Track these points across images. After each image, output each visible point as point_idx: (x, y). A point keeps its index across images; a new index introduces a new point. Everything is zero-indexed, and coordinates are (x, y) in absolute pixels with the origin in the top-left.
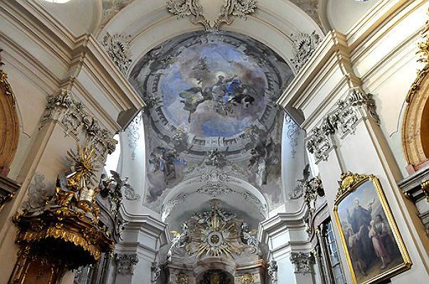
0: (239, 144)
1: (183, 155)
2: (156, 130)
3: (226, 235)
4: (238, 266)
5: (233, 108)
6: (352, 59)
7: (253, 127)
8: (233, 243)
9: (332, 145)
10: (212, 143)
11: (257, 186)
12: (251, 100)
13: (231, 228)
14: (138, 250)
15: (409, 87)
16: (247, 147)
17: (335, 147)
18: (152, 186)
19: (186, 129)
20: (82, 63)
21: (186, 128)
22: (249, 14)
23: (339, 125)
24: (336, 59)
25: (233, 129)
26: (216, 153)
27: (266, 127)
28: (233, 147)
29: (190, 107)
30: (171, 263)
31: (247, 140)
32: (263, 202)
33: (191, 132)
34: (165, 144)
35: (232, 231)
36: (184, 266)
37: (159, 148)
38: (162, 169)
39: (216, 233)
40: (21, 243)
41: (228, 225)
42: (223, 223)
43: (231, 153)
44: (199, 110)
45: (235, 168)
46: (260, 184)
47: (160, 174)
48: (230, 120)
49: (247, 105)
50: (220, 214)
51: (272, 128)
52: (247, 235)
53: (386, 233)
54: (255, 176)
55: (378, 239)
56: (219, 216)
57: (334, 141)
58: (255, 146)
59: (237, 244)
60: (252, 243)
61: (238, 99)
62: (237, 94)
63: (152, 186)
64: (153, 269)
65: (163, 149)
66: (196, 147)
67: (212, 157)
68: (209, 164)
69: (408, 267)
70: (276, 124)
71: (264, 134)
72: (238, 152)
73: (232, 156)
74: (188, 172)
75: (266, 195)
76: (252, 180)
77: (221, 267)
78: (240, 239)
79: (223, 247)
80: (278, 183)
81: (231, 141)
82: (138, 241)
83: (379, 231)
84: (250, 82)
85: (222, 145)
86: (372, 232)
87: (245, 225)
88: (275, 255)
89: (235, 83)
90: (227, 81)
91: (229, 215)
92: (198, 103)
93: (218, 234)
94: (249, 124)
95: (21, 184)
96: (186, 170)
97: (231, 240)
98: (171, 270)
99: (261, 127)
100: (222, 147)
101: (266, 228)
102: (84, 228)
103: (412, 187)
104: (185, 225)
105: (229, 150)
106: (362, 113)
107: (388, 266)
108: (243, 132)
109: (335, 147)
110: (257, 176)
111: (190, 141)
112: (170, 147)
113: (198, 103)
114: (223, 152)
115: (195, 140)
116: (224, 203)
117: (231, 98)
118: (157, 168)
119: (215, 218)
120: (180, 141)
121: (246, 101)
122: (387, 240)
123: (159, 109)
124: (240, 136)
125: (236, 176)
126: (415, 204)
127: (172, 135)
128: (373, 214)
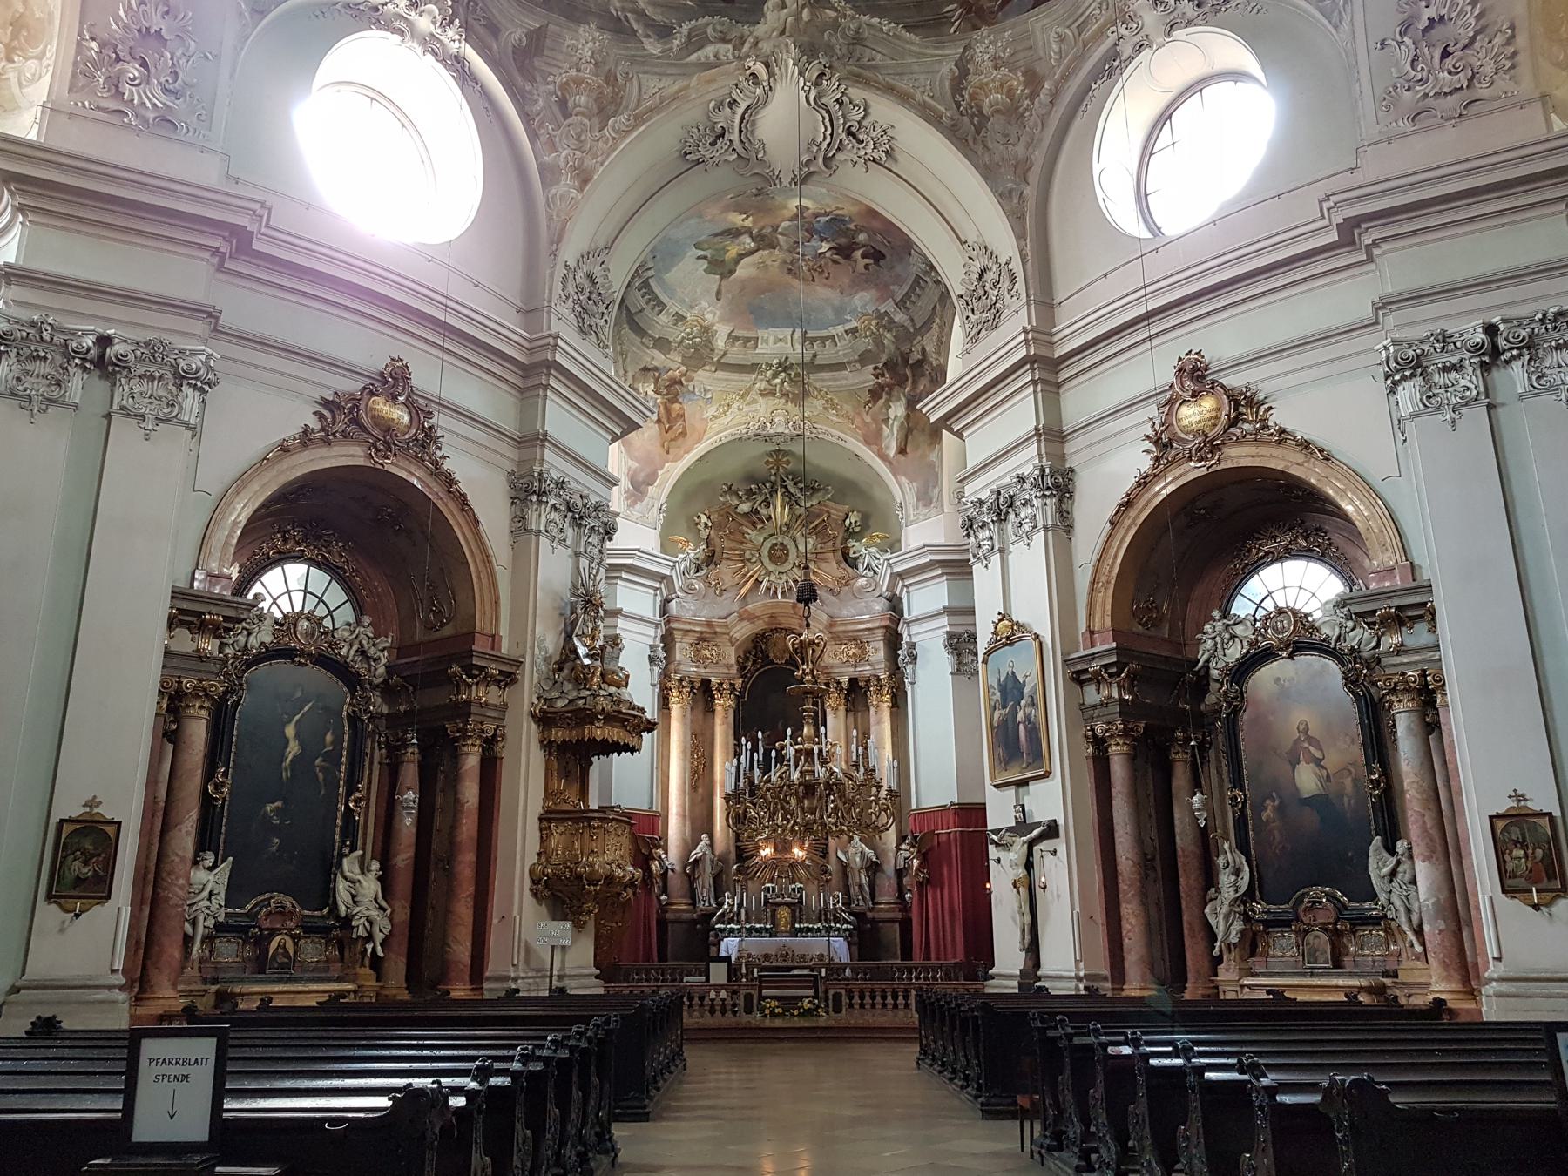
0: (842, 350)
5: (832, 268)
8: (823, 565)
15: (1118, 497)
24: (1030, 378)
40: (547, 745)
53: (1034, 724)
55: (1025, 727)
69: (1047, 775)
83: (1028, 718)
95: (524, 657)
102: (628, 720)
103: (1079, 667)
106: (1045, 518)
122: (1033, 731)
125: (834, 425)
126: (1082, 688)
128: (1026, 691)
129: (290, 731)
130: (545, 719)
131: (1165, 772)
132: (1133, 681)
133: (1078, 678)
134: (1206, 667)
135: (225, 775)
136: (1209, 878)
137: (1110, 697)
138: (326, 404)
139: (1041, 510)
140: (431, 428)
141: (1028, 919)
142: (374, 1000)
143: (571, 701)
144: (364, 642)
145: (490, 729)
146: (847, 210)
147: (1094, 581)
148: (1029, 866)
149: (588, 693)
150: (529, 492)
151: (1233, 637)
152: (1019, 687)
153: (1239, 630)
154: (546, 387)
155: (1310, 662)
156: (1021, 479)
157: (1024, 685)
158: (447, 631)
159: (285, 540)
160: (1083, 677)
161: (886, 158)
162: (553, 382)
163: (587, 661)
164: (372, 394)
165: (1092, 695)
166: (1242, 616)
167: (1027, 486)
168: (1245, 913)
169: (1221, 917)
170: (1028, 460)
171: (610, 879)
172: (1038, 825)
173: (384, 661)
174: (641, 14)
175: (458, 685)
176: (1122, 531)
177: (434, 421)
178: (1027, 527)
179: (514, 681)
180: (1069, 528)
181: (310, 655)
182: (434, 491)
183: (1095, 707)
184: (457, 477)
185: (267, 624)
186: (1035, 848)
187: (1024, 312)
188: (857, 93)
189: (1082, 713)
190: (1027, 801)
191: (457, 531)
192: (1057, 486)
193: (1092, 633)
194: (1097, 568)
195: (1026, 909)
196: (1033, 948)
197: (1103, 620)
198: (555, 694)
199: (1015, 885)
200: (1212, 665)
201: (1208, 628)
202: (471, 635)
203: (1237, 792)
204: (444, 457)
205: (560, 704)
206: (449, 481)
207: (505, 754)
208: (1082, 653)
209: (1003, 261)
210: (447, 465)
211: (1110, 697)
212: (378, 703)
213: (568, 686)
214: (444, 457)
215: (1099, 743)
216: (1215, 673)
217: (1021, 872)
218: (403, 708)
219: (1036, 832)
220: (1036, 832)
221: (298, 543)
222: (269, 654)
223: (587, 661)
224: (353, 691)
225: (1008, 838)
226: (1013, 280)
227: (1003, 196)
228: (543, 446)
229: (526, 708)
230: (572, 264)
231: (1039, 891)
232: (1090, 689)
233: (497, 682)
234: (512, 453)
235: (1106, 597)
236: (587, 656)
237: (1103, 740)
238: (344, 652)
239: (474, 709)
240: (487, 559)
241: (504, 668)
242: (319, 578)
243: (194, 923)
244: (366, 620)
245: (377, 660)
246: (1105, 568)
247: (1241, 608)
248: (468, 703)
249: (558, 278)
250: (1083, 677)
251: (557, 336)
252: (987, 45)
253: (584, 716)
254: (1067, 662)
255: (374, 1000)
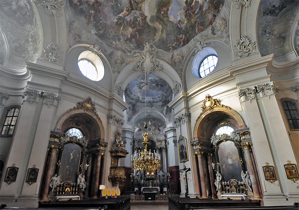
1: (138, 104)
2: (129, 97)
3: (153, 128)
4: (157, 139)
6: (188, 99)
7: (163, 95)
9: (179, 125)
10: (148, 99)
11: (163, 115)
12: (162, 86)
13: (154, 125)
14: (126, 139)
16: (161, 101)
17: (180, 126)
18: (129, 116)
19: (139, 95)
20: (113, 102)
21: (139, 95)
22: (161, 70)
23: (181, 120)
24: (183, 99)
25: (155, 94)
26: (150, 102)
27: (167, 95)
28: (155, 100)
29: (140, 88)
30: (135, 139)
31: (160, 99)
32: (166, 120)
33: (141, 96)
34: (132, 101)
35: (155, 126)
36: (140, 139)
37: (130, 103)
38: (131, 109)
39: (150, 127)
40: (112, 156)
41: (154, 124)
42: (152, 123)
43: (155, 102)
44: (143, 88)
45: (156, 108)
46: (165, 114)
47: (131, 111)
48: (154, 92)
49: (160, 87)
50: (151, 120)
51: (169, 95)
52: (161, 128)
54: (163, 111)
56: (151, 121)
57: (180, 124)
58: (163, 101)
59: (157, 131)
60: (162, 131)
61: (157, 85)
62: (157, 84)
63: (129, 116)
64: (131, 144)
65: (131, 102)
66: (143, 101)
67: (148, 103)
68: (147, 106)
69: (188, 161)
70: (171, 95)
71: (167, 97)
72: (157, 102)
73: (155, 103)
74: (140, 109)
75: (167, 118)
76: (162, 112)
77: (152, 139)
78: (158, 129)
79: (152, 132)
80: (171, 114)
81: (155, 98)
82: (126, 136)
83: (185, 151)
84: (161, 81)
85: (152, 99)
86: (184, 151)
87: (160, 124)
88: (168, 139)
89: (156, 81)
90: (153, 80)
91: (155, 120)
92: (143, 86)
93: (150, 127)
94: (161, 94)
96: (139, 109)
97: (155, 129)
98: (135, 141)
99: (165, 95)
100: (152, 100)
101: (166, 131)
103: (193, 143)
104: (139, 124)
105: (155, 101)
107: (186, 159)
108: (159, 96)
109: (180, 126)
110: (164, 111)
111: (141, 99)
112: (134, 102)
113: (143, 86)
114: (152, 102)
115: (142, 98)
116: (153, 116)
117: (154, 85)
118: (130, 109)
119: (149, 122)
120: (137, 99)
121: (160, 86)
122: (186, 153)
123: (130, 90)
124: (158, 97)
127: (135, 97)
128: (185, 147)
129: (71, 154)
130: (111, 152)
131: (207, 160)
132: (201, 145)
133: (193, 145)
134: (212, 143)
135: (60, 161)
136: (215, 178)
137: (197, 148)
138: (79, 103)
139: (186, 119)
140: (94, 107)
141: (186, 184)
142: (79, 199)
143: (115, 149)
144: (84, 141)
145: (102, 154)
146: (157, 79)
147: (194, 130)
148: (186, 175)
149: (117, 148)
150: (110, 117)
151: (216, 138)
152: (184, 147)
153: (217, 137)
154: (113, 102)
155: (229, 142)
156: (183, 115)
157: (184, 146)
158: (97, 138)
159: (72, 125)
160: (193, 145)
161: (162, 69)
162: (114, 101)
163: (118, 143)
164: (85, 102)
165: (195, 148)
166: (217, 135)
167: (183, 116)
168: (221, 184)
169: (217, 184)
170: (184, 112)
171: (121, 178)
172: (187, 169)
173: (87, 143)
174: (127, 49)
175: (98, 147)
176: (198, 122)
177: (95, 106)
178: (184, 122)
179: (107, 146)
180: (190, 122)
181: (75, 142)
182: (95, 117)
183: (195, 149)
184: (98, 115)
185: (69, 138)
186: (187, 173)
187: (182, 90)
188: (158, 60)
189: (193, 151)
190: (185, 165)
191: (98, 123)
192: (188, 115)
193: (194, 138)
194: (195, 127)
195: (186, 183)
196: (187, 190)
197: (196, 136)
198: (113, 148)
199: (184, 179)
200: (213, 143)
201: (212, 137)
202: (100, 139)
203: (218, 163)
204: (96, 112)
205: (114, 150)
206: (97, 115)
207: (105, 157)
208: (193, 141)
209: (179, 83)
210: (97, 113)
211: (197, 148)
212: (86, 150)
213: (115, 147)
214: (96, 112)
215: (196, 155)
216: (214, 144)
217: (185, 177)
218: (90, 151)
219: (187, 170)
220: (187, 170)
221: (74, 125)
222: (68, 142)
223: (118, 143)
224: (82, 148)
225: (183, 171)
226: (181, 86)
227: (179, 74)
228: (112, 111)
229: (108, 150)
230: (117, 85)
231: (188, 180)
232: (194, 147)
233: (104, 146)
234: (107, 111)
235: (196, 132)
236: (118, 142)
237: (197, 155)
238: (81, 142)
239: (100, 151)
240: (103, 127)
241: (105, 144)
242: (78, 131)
243: (53, 186)
244: (85, 137)
245: (86, 143)
246: (196, 128)
247: (217, 134)
248: (99, 149)
249: (115, 87)
250: (193, 145)
251: (114, 94)
252: (176, 52)
253: (117, 152)
254: (191, 143)
255: (79, 199)
